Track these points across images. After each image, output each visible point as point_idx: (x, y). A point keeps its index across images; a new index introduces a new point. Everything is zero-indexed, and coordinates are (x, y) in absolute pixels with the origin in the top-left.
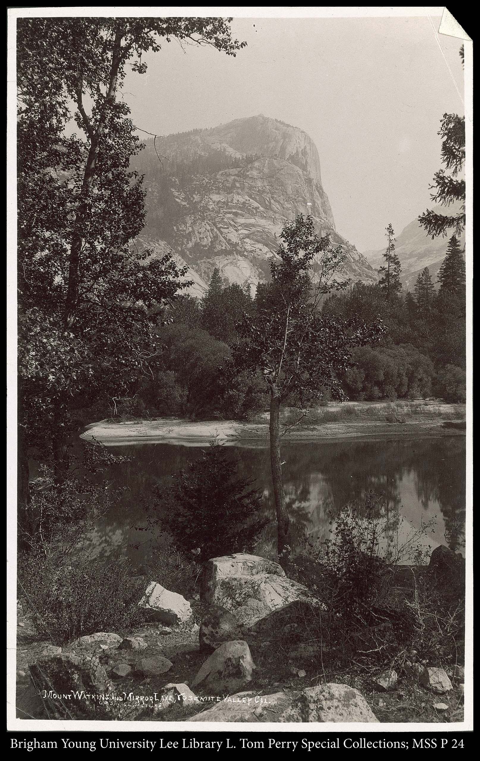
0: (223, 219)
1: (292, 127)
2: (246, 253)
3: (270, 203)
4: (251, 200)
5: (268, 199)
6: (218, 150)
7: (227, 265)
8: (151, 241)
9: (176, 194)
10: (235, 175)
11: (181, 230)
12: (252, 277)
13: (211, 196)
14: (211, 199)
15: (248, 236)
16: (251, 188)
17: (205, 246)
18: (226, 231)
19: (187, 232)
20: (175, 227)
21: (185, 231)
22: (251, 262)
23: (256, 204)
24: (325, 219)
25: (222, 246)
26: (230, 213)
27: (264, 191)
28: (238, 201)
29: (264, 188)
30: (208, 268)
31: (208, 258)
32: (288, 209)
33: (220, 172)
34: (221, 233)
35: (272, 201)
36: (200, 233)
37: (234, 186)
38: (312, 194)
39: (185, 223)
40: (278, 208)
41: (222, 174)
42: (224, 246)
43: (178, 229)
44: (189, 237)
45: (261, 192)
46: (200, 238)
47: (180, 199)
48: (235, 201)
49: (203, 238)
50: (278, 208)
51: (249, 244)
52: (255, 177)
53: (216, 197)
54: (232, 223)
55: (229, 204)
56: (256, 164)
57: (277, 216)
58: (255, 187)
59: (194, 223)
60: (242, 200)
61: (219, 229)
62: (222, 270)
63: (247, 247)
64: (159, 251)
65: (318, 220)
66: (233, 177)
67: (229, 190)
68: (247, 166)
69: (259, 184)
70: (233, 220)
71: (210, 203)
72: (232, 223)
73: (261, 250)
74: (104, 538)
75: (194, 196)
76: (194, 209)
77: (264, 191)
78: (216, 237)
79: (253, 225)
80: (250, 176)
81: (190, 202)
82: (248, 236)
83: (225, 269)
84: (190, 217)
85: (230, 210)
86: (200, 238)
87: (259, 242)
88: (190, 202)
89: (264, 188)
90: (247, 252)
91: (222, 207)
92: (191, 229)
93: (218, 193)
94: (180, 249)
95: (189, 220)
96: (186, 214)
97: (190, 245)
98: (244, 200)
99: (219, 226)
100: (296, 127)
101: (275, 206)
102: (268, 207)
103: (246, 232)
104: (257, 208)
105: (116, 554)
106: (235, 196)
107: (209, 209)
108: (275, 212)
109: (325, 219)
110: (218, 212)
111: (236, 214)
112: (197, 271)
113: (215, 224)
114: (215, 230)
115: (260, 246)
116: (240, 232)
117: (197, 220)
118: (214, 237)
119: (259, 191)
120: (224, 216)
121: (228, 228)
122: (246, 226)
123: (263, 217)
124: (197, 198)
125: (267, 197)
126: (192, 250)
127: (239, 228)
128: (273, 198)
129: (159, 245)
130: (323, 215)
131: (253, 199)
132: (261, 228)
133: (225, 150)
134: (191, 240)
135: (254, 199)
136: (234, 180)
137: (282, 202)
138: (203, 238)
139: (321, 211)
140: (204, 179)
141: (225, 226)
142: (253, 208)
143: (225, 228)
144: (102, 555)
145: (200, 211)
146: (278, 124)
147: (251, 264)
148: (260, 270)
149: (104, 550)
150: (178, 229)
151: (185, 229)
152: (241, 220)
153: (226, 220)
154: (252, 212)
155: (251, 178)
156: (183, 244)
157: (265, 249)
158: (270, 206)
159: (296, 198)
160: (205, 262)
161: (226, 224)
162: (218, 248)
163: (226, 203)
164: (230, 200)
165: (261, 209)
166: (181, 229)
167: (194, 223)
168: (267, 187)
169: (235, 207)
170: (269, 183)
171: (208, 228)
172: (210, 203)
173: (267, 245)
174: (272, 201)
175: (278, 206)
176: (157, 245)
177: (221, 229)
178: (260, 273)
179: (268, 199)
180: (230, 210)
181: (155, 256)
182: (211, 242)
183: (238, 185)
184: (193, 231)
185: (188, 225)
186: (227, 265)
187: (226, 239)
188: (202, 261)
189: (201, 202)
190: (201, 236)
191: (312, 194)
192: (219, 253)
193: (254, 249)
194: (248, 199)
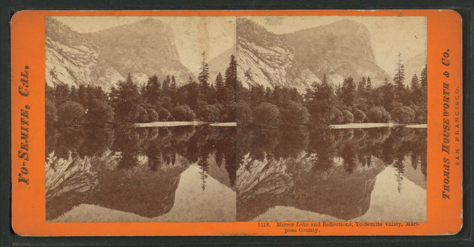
19: (122, 64)
74: (91, 182)
105: (96, 188)
113: (133, 61)
114: (133, 63)
144: (91, 188)
149: (91, 187)
171: (130, 62)
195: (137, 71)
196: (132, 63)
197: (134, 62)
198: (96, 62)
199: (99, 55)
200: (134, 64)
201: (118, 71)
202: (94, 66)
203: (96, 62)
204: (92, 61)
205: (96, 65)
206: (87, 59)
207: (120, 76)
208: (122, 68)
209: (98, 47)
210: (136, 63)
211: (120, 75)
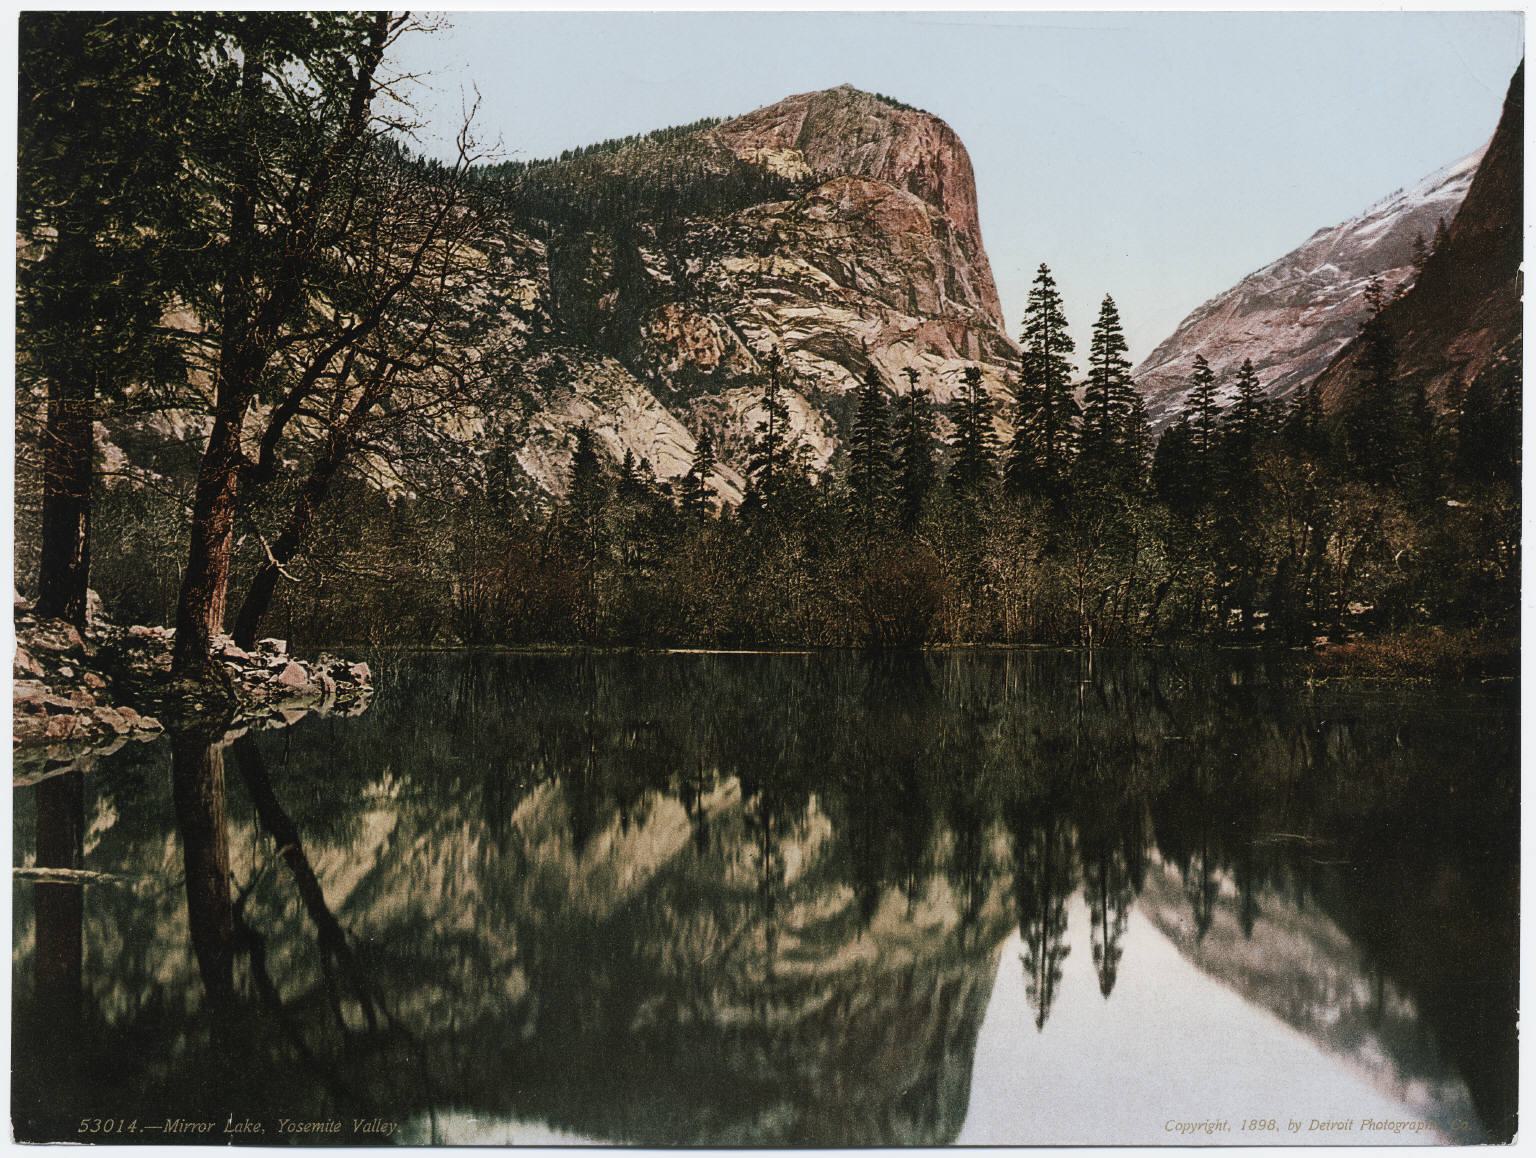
0: (749, 309)
1: (915, 110)
2: (797, 382)
3: (853, 273)
4: (812, 268)
5: (849, 265)
6: (752, 162)
7: (754, 406)
8: (585, 359)
9: (648, 258)
10: (778, 216)
11: (657, 335)
12: (807, 430)
13: (725, 262)
14: (724, 268)
15: (802, 345)
16: (811, 241)
17: (707, 367)
18: (755, 334)
19: (669, 338)
20: (643, 329)
21: (664, 335)
22: (808, 399)
23: (823, 277)
24: (977, 307)
25: (744, 367)
26: (764, 296)
27: (840, 250)
28: (783, 270)
29: (841, 242)
30: (712, 415)
31: (712, 392)
32: (892, 286)
33: (746, 211)
34: (744, 339)
35: (858, 270)
36: (696, 340)
37: (774, 240)
38: (946, 254)
39: (665, 320)
40: (870, 285)
41: (750, 214)
42: (749, 366)
43: (649, 331)
44: (671, 348)
45: (834, 252)
46: (697, 351)
47: (655, 269)
48: (776, 272)
49: (703, 350)
50: (870, 285)
51: (803, 362)
52: (823, 219)
53: (734, 264)
54: (769, 317)
55: (764, 276)
56: (825, 192)
57: (868, 300)
58: (822, 240)
59: (685, 319)
60: (790, 267)
61: (739, 331)
62: (742, 418)
63: (800, 369)
64: (601, 380)
65: (961, 308)
66: (773, 220)
67: (764, 249)
68: (804, 196)
69: (830, 232)
70: (770, 312)
71: (723, 276)
72: (769, 317)
73: (831, 373)
75: (688, 261)
76: (685, 289)
77: (840, 250)
78: (731, 349)
79: (815, 322)
80: (811, 217)
81: (679, 276)
82: (802, 345)
83: (749, 414)
84: (676, 306)
85: (765, 291)
86: (697, 351)
87: (827, 358)
88: (679, 276)
89: (841, 242)
90: (801, 378)
91: (748, 285)
92: (676, 332)
93: (740, 255)
94: (651, 374)
95: (673, 312)
96: (669, 301)
97: (674, 366)
98: (795, 269)
99: (741, 323)
100: (923, 111)
101: (865, 280)
102: (848, 282)
103: (800, 336)
104: (823, 285)
106: (776, 259)
107: (718, 290)
108: (864, 293)
109: (977, 307)
110: (739, 295)
111: (778, 299)
112: (686, 422)
113: (730, 321)
114: (730, 332)
115: (830, 365)
116: (786, 336)
117: (692, 312)
118: (728, 348)
119: (829, 249)
120: (751, 302)
121: (759, 328)
122: (799, 323)
123: (837, 304)
124: (693, 265)
125: (846, 260)
126: (677, 377)
127: (785, 327)
128: (860, 263)
129: (603, 367)
130: (972, 298)
131: (816, 265)
132: (832, 327)
133: (765, 160)
134: (676, 355)
135: (820, 266)
136: (776, 226)
137: (879, 270)
138: (703, 350)
139: (968, 288)
140: (710, 226)
141: (754, 325)
142: (815, 285)
143: (753, 329)
145: (700, 293)
146: (882, 105)
147: (809, 405)
148: (828, 418)
150: (649, 331)
151: (664, 331)
152: (789, 312)
153: (754, 311)
154: (813, 295)
155: (813, 221)
156: (658, 362)
157: (841, 372)
158: (853, 279)
159: (910, 261)
160: (705, 402)
161: (755, 319)
162: (736, 370)
163: (756, 276)
164: (764, 269)
165: (834, 285)
166: (655, 331)
167: (685, 319)
168: (848, 239)
169: (774, 284)
170: (852, 230)
171: (715, 328)
172: (723, 276)
173: (845, 364)
174: (858, 270)
175: (871, 280)
176: (597, 367)
177: (746, 332)
178: (828, 424)
179: (849, 265)
180: (765, 291)
181: (593, 390)
182: (721, 359)
183: (783, 236)
184: (683, 335)
185: (671, 323)
186: (754, 406)
187: (752, 350)
188: (699, 399)
189: (700, 274)
190: (699, 346)
191: (946, 254)
192: (739, 381)
193: (816, 371)
194: (805, 265)
195: (751, 375)
196: (723, 333)
197: (734, 327)
198: (522, 327)
199: (539, 288)
200: (736, 338)
201: (641, 378)
202: (509, 348)
203: (522, 327)
204: (504, 323)
205: (521, 344)
206: (473, 313)
207: (650, 407)
208: (671, 362)
209: (540, 248)
210: (746, 332)
211: (652, 398)
